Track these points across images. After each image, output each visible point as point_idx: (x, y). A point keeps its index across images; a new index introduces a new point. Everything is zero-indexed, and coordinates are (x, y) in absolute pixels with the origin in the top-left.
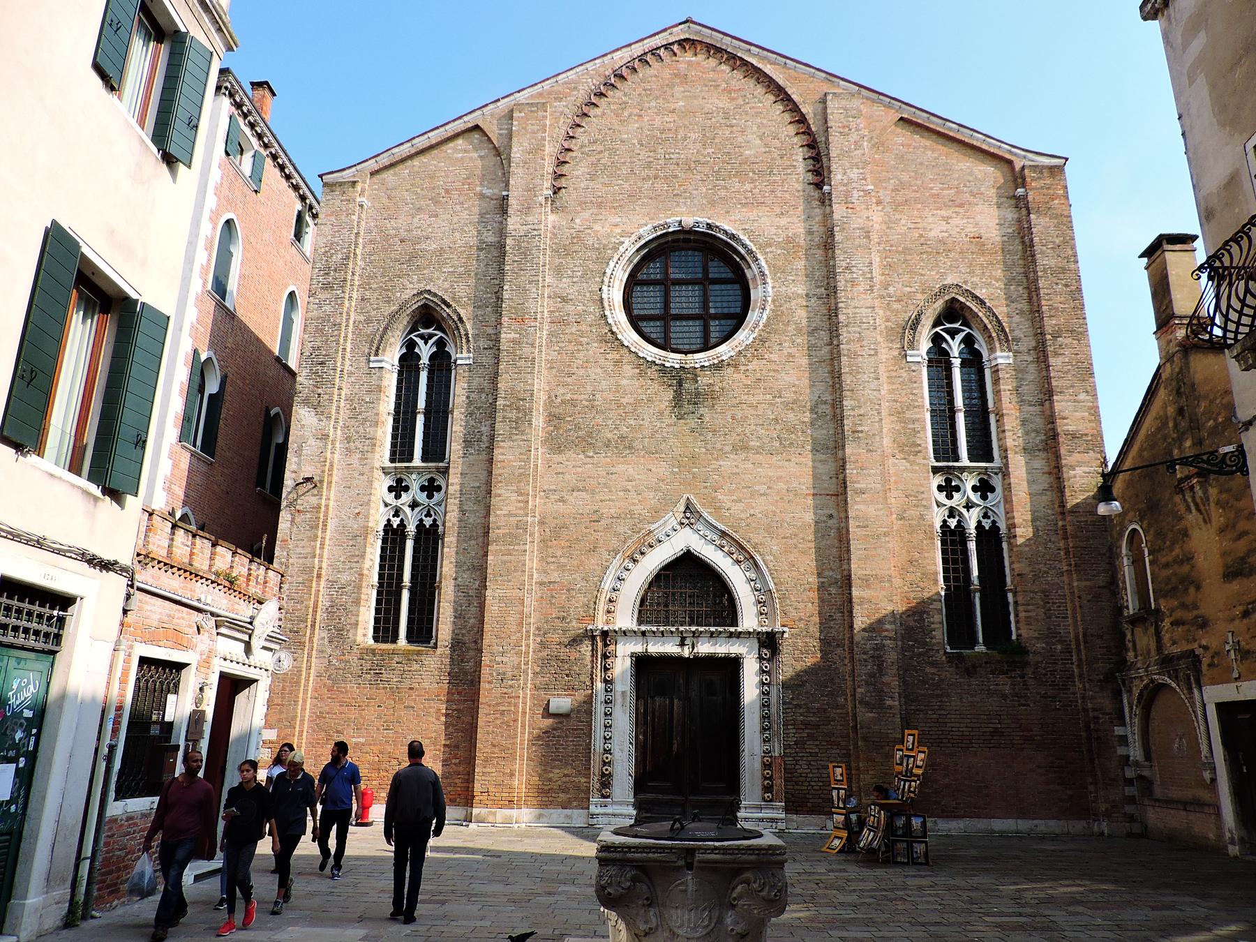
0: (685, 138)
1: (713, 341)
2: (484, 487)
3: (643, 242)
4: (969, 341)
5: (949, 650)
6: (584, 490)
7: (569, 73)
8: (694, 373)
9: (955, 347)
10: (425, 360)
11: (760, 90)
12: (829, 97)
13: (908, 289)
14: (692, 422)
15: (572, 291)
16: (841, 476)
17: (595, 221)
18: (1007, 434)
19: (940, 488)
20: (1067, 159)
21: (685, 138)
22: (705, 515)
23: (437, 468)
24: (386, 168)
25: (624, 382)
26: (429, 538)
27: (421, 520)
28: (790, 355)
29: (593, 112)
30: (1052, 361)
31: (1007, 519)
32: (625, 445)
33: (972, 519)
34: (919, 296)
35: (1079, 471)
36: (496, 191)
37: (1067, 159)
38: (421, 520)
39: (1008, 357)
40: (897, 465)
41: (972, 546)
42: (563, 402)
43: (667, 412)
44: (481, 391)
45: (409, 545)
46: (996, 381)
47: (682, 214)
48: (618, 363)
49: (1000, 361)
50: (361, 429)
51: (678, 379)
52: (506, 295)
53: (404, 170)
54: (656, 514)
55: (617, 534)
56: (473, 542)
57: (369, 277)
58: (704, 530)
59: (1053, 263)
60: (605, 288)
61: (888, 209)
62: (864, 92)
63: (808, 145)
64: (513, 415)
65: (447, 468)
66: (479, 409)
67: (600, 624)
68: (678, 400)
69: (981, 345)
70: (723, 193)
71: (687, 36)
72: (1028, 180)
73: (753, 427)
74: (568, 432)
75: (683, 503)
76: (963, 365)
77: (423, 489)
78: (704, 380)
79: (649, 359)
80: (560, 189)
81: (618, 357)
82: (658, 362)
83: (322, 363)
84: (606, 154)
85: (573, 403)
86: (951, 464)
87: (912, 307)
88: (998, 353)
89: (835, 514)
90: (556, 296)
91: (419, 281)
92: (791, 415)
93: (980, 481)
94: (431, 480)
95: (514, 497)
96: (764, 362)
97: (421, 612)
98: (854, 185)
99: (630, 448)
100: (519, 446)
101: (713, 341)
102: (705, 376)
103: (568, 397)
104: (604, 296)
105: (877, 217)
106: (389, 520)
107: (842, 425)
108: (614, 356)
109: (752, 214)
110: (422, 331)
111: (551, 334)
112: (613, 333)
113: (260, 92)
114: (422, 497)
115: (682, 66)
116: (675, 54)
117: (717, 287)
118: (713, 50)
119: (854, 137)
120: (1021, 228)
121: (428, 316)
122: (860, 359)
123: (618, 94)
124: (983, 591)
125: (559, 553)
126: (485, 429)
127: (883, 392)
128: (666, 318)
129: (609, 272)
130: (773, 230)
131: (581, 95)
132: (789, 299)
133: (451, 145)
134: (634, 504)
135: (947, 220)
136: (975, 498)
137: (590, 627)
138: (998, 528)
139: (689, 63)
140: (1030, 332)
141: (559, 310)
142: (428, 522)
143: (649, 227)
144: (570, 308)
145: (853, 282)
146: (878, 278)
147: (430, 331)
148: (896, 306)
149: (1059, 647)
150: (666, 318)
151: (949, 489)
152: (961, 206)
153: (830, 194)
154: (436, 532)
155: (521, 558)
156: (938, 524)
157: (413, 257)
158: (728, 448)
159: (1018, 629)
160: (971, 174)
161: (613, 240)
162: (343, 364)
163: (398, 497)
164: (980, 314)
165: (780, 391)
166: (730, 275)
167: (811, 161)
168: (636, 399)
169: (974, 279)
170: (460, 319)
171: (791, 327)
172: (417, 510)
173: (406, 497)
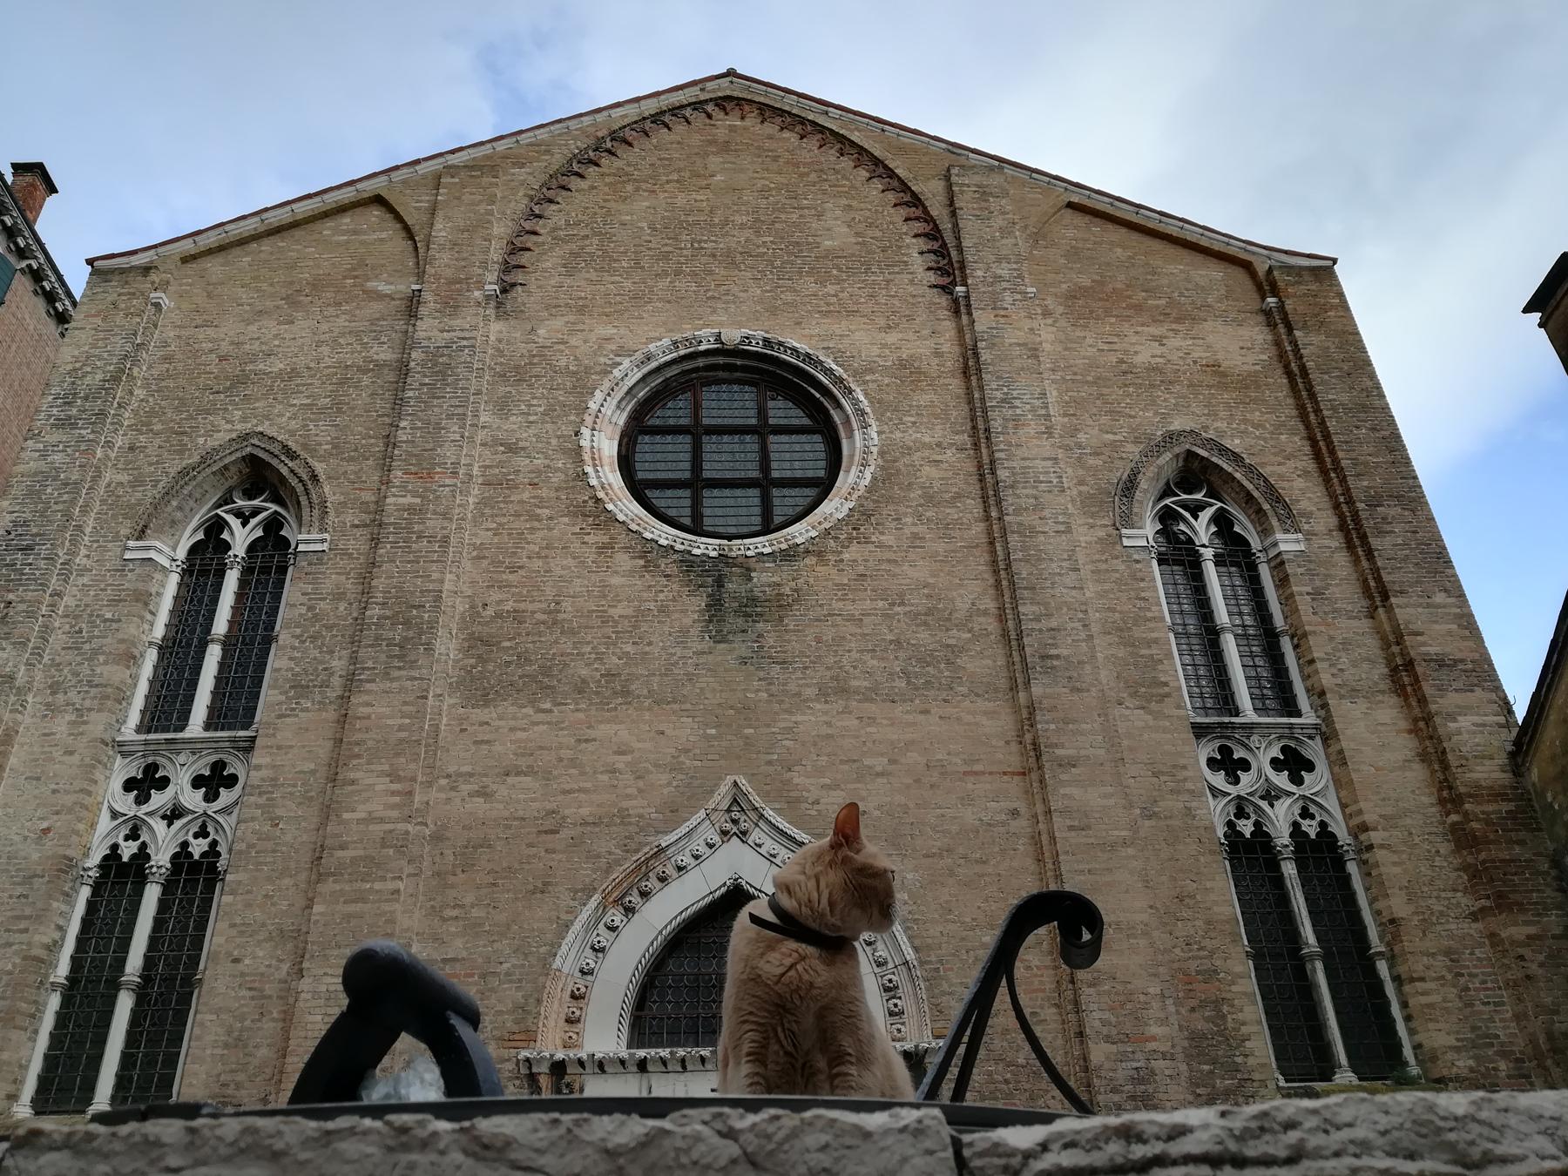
0: (726, 222)
1: (777, 520)
2: (323, 772)
3: (654, 365)
4: (1222, 522)
5: (1282, 1083)
6: (530, 771)
7: (537, 132)
8: (745, 568)
9: (1202, 529)
10: (239, 548)
11: (846, 163)
12: (954, 171)
13: (1111, 437)
14: (741, 647)
15: (527, 436)
16: (1028, 737)
17: (572, 332)
18: (1319, 665)
19: (1211, 762)
20: (1335, 261)
21: (726, 222)
22: (769, 813)
23: (233, 740)
24: (210, 252)
25: (616, 581)
26: (196, 877)
27: (185, 845)
28: (915, 536)
29: (575, 183)
30: (1375, 542)
31: (1347, 817)
32: (615, 690)
33: (1280, 819)
34: (1130, 447)
35: (1465, 722)
36: (402, 287)
37: (1335, 261)
38: (185, 845)
39: (1298, 541)
40: (1131, 718)
41: (1289, 869)
42: (498, 615)
43: (694, 632)
44: (339, 596)
45: (152, 895)
46: (1283, 582)
47: (721, 324)
48: (603, 548)
49: (1283, 547)
50: (85, 670)
51: (712, 578)
52: (402, 436)
53: (243, 259)
54: (673, 814)
55: (593, 856)
56: (287, 881)
57: (152, 413)
58: (769, 845)
59: (1344, 398)
60: (586, 432)
61: (1063, 323)
62: (1008, 170)
63: (926, 235)
64: (398, 633)
65: (253, 739)
66: (329, 628)
67: (550, 1045)
68: (715, 606)
69: (1244, 526)
70: (789, 297)
71: (728, 93)
72: (1281, 284)
73: (855, 655)
74: (507, 664)
75: (725, 788)
76: (1219, 561)
77: (197, 782)
78: (763, 578)
79: (663, 542)
80: (514, 285)
81: (606, 539)
82: (678, 547)
83: (29, 548)
84: (595, 241)
85: (518, 616)
86: (1226, 720)
87: (1119, 464)
88: (1279, 536)
89: (1023, 810)
90: (497, 442)
91: (244, 419)
92: (923, 635)
93: (1284, 749)
94: (219, 766)
95: (383, 784)
96: (871, 547)
97: (153, 1041)
98: (1005, 285)
99: (625, 693)
100: (401, 690)
101: (777, 520)
102: (766, 570)
103: (509, 606)
104: (585, 443)
105: (1047, 336)
106: (115, 847)
107: (1022, 648)
108: (598, 537)
109: (840, 327)
110: (240, 503)
111: (483, 502)
112: (598, 500)
113: (28, 178)
114: (193, 800)
115: (721, 133)
116: (709, 116)
117: (784, 438)
118: (767, 111)
119: (998, 222)
120: (1282, 355)
121: (259, 476)
122: (1042, 538)
123: (618, 163)
124: (1327, 959)
125: (469, 899)
126: (339, 664)
127: (1088, 594)
128: (697, 484)
129: (593, 406)
130: (875, 350)
131: (557, 160)
132: (908, 450)
133: (330, 223)
134: (629, 797)
135: (1160, 340)
136: (1281, 780)
137: (524, 1054)
138: (1333, 835)
139: (732, 129)
140: (1326, 503)
141: (501, 464)
142: (198, 847)
143: (666, 342)
144: (522, 462)
145: (1017, 422)
146: (1058, 420)
147: (256, 502)
148: (1091, 461)
149: (1503, 1065)
150: (697, 484)
151: (1230, 765)
152: (1178, 320)
153: (967, 297)
154: (212, 868)
155: (386, 907)
156: (1221, 831)
157: (241, 380)
158: (810, 692)
159: (1412, 1032)
160: (1188, 280)
161: (602, 360)
162: (72, 553)
163: (142, 800)
164: (1238, 475)
165: (901, 595)
166: (806, 421)
167: (932, 257)
168: (638, 610)
169: (1216, 425)
170: (314, 477)
171: (916, 494)
172: (178, 824)
173: (158, 799)
